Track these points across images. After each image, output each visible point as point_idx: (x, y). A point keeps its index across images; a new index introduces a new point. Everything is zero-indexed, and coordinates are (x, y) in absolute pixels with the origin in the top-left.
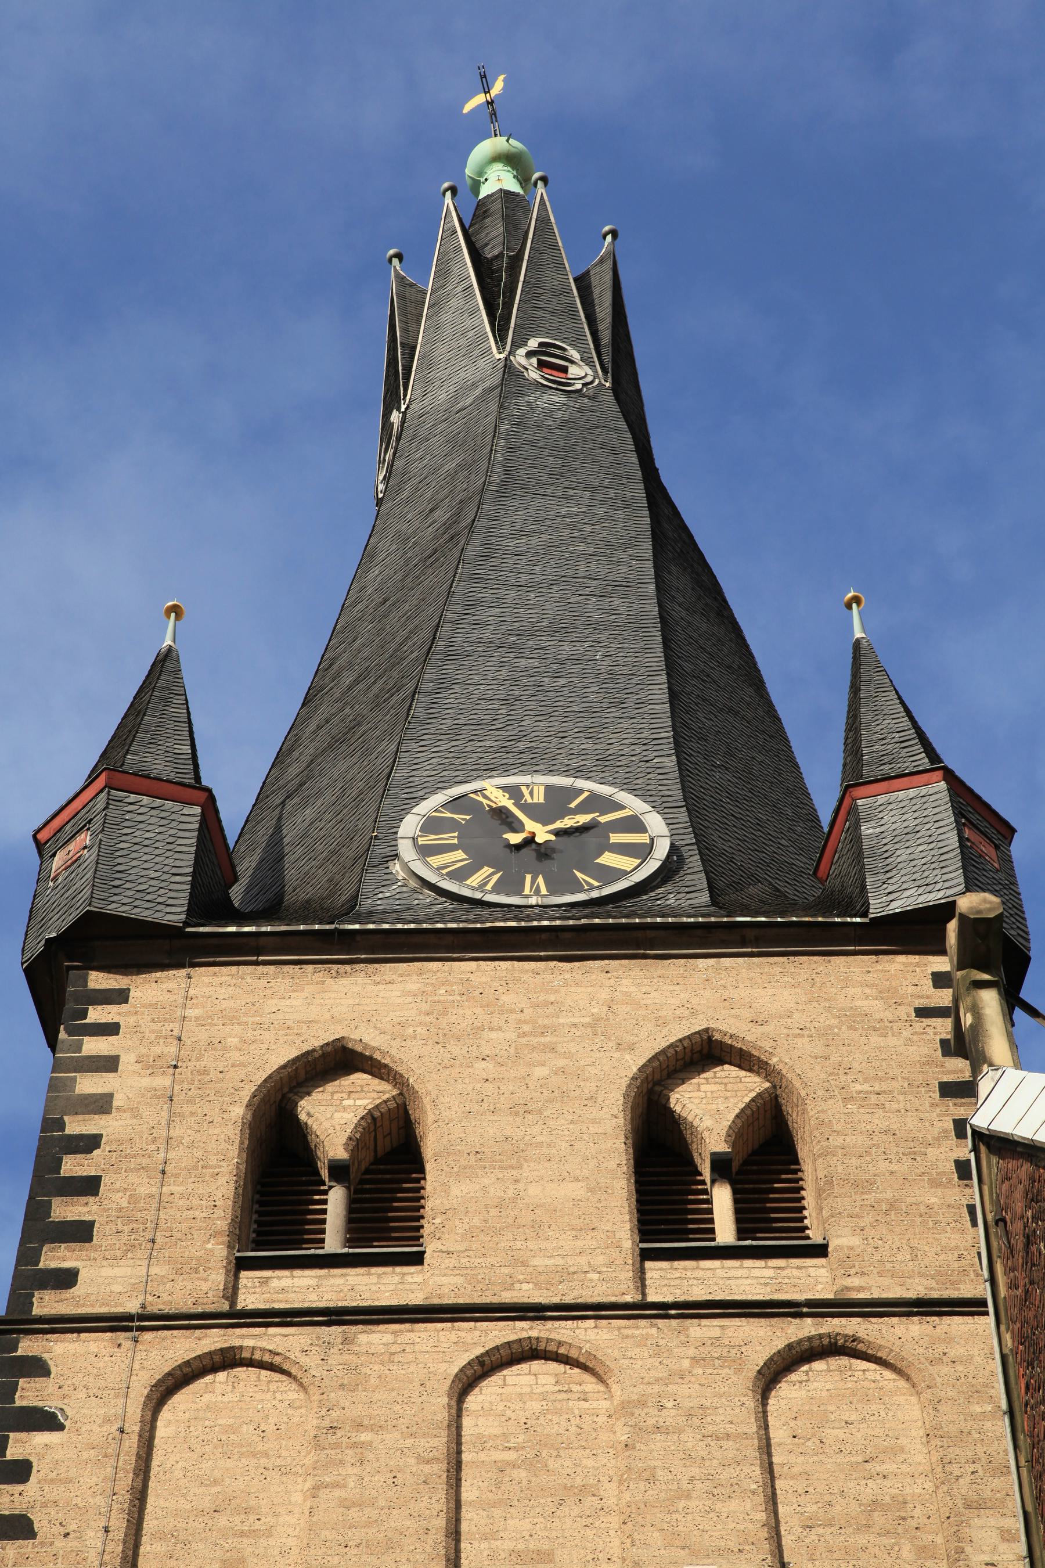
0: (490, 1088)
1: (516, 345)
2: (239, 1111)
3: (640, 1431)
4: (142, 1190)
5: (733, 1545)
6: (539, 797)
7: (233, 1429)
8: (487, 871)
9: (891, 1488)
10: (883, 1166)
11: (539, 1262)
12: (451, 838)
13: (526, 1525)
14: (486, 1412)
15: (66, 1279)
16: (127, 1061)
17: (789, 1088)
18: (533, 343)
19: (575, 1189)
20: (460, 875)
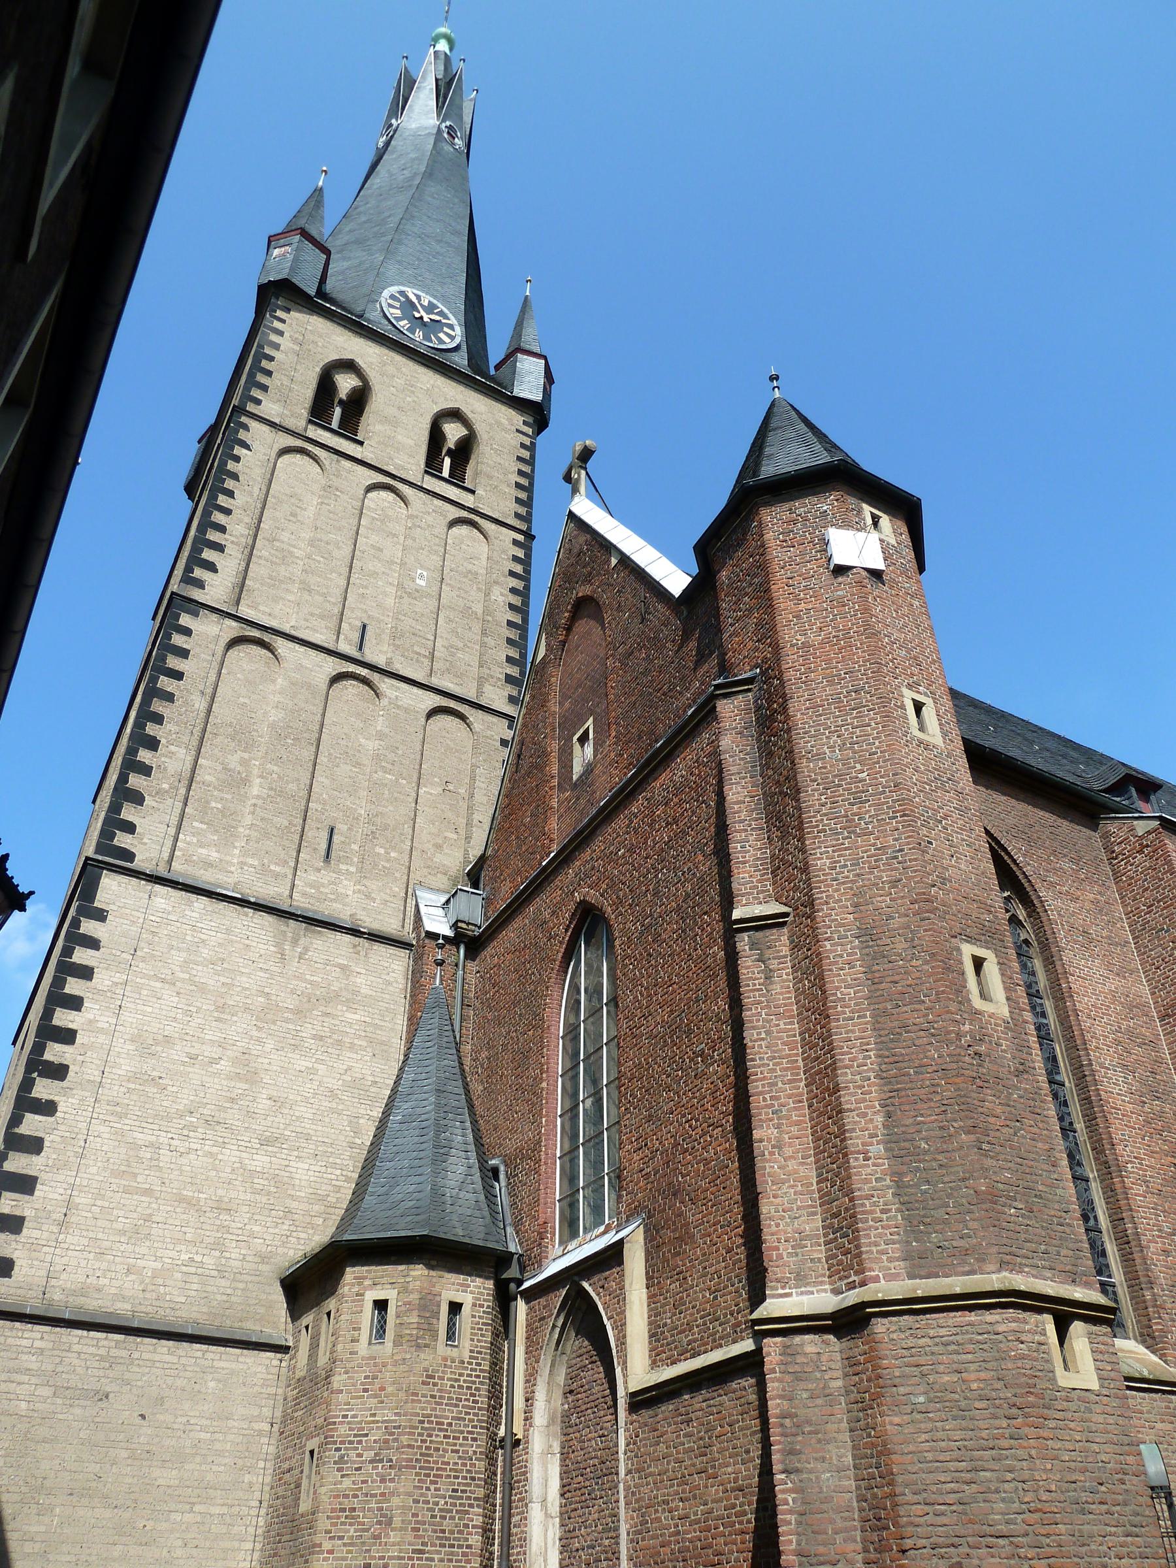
0: (393, 397)
1: (443, 121)
2: (318, 369)
3: (414, 525)
5: (432, 568)
6: (426, 303)
8: (406, 322)
9: (475, 569)
10: (496, 474)
12: (397, 304)
13: (377, 538)
14: (372, 500)
15: (258, 402)
17: (476, 437)
18: (448, 123)
19: (412, 443)
20: (398, 319)
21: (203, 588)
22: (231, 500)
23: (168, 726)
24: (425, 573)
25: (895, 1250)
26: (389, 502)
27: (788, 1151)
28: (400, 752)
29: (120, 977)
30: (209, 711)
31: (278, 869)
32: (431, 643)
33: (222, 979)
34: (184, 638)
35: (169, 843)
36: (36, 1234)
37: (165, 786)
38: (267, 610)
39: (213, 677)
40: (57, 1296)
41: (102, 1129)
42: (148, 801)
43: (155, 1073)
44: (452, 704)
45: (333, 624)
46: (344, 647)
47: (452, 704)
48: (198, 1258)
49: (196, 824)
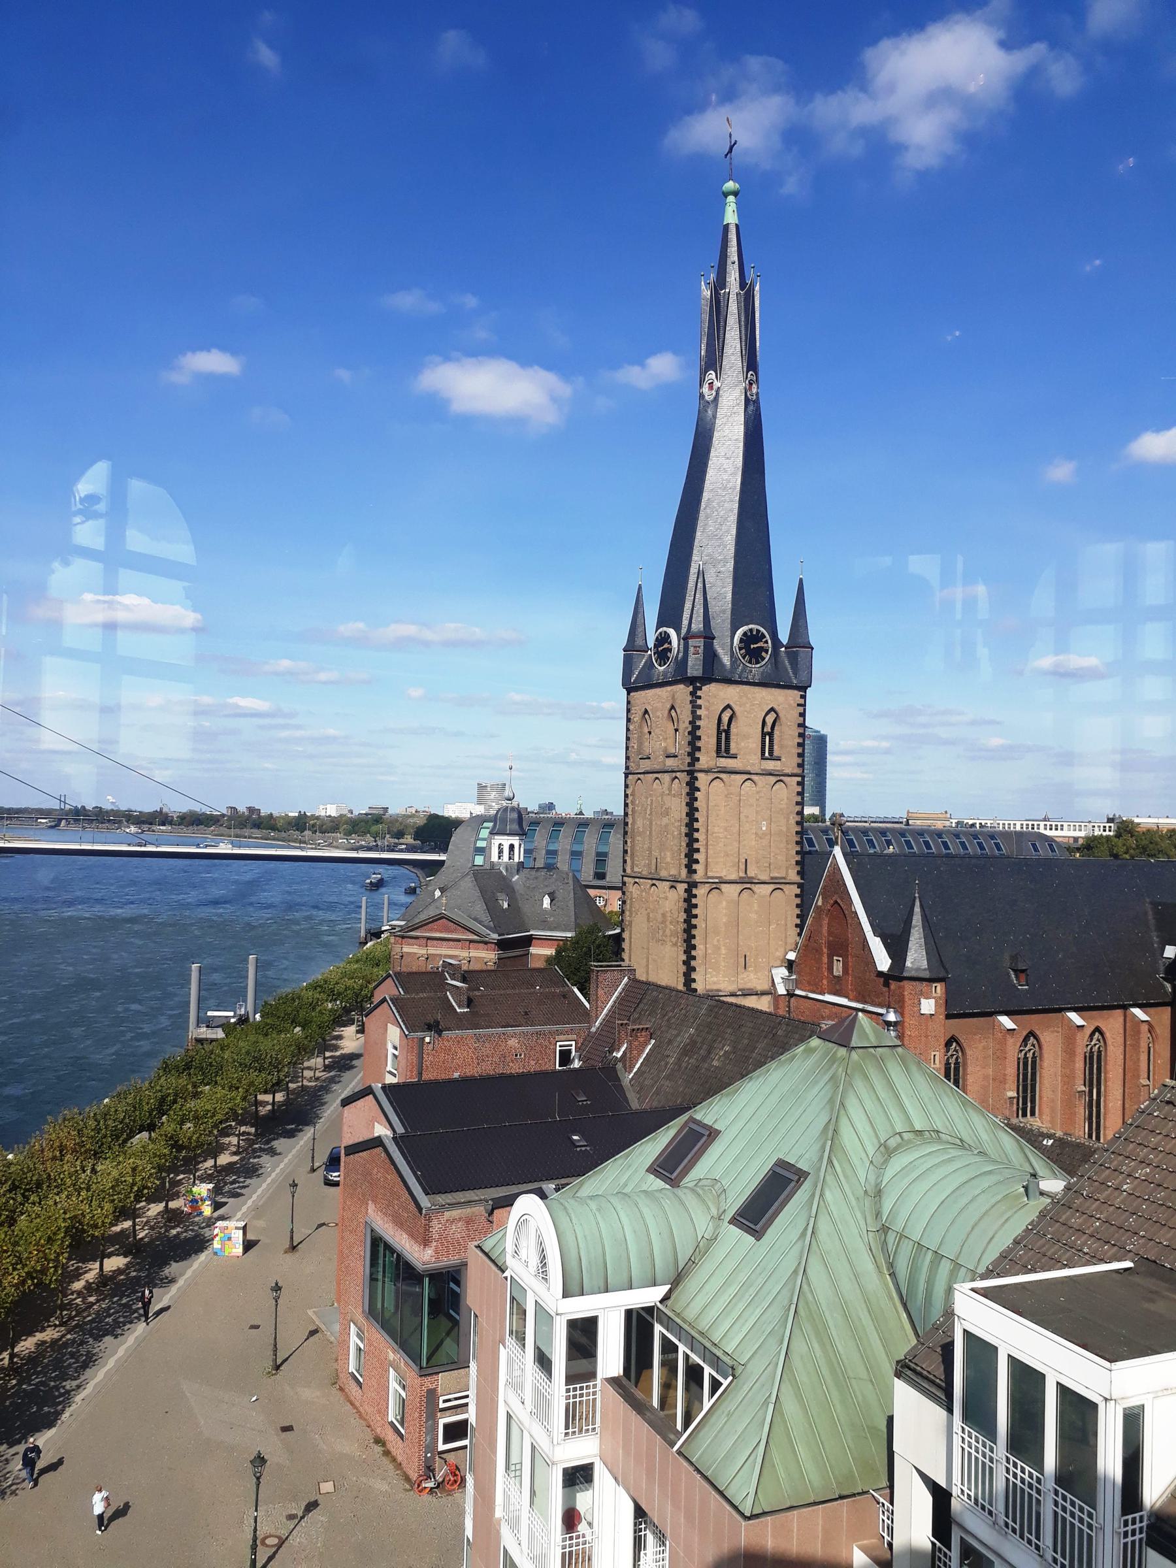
23: (697, 938)
42: (697, 969)
44: (778, 886)
47: (778, 886)
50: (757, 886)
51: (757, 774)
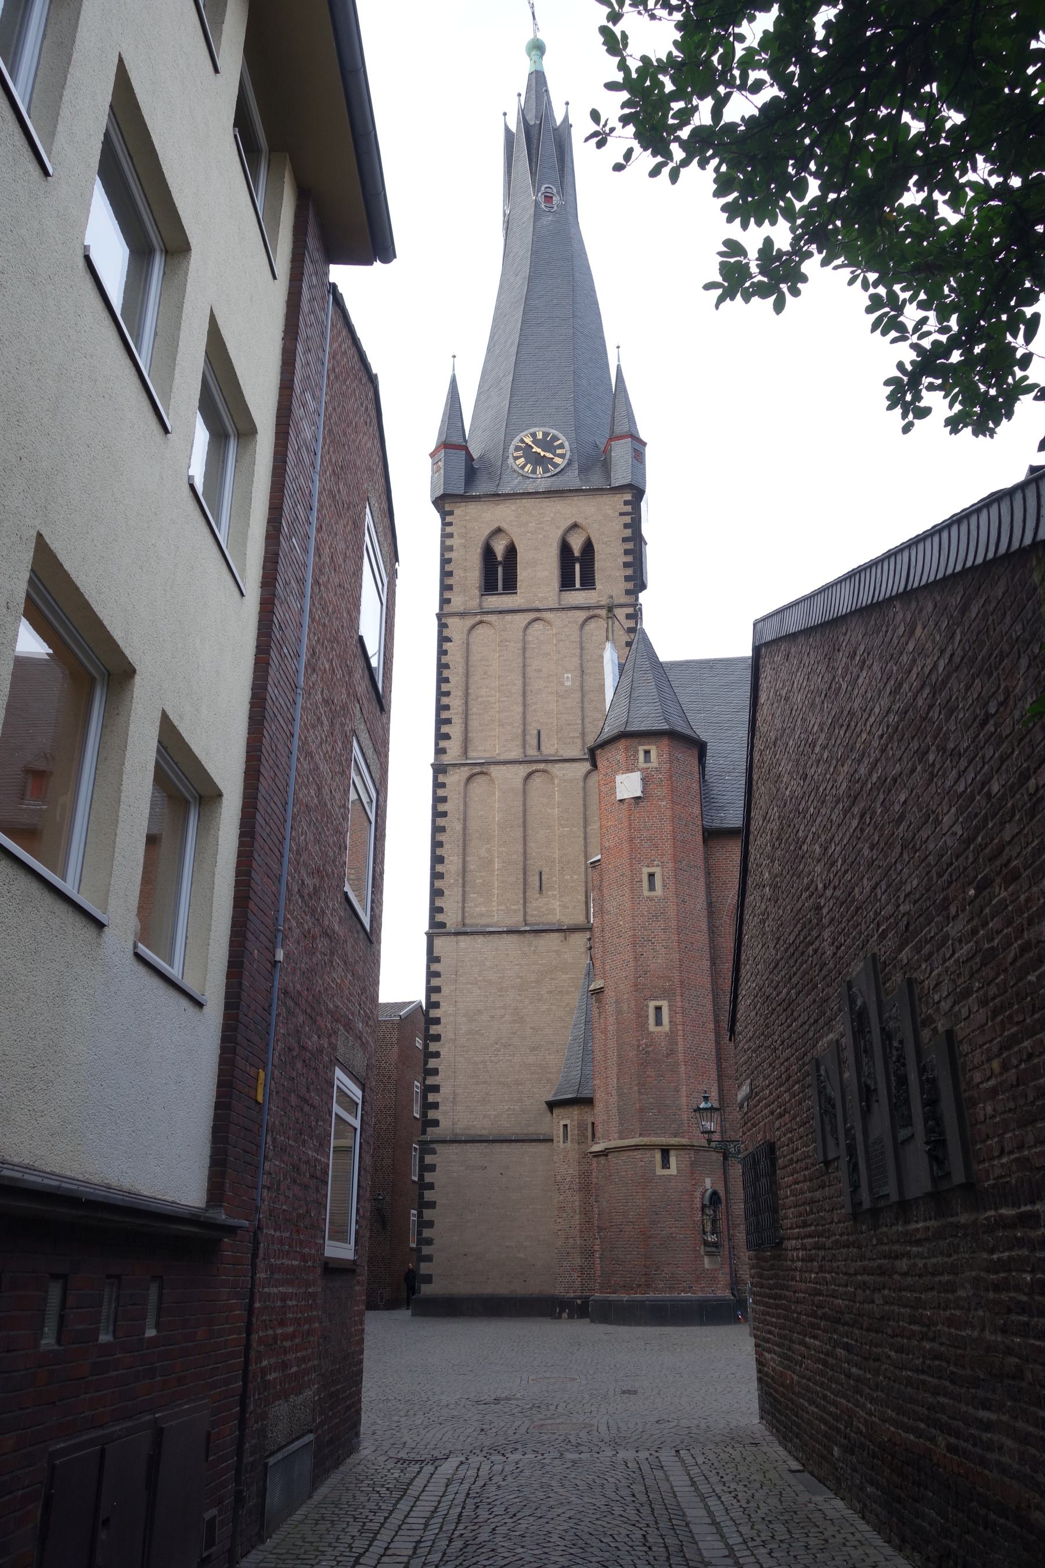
2: (479, 550)
3: (558, 641)
4: (462, 575)
7: (483, 640)
8: (529, 465)
11: (540, 595)
12: (520, 453)
16: (455, 534)
19: (547, 573)
21: (445, 752)
22: (448, 685)
23: (446, 846)
24: (570, 675)
25: (616, 1129)
26: (540, 630)
27: (602, 1089)
28: (571, 811)
29: (453, 987)
30: (465, 828)
31: (515, 907)
32: (580, 726)
33: (498, 975)
34: (443, 789)
35: (460, 912)
36: (444, 1108)
37: (452, 881)
38: (483, 748)
39: (462, 808)
40: (459, 1131)
41: (461, 1059)
42: (446, 893)
43: (477, 1029)
45: (519, 742)
46: (532, 752)
48: (512, 1107)
49: (472, 895)
50: (558, 766)
51: (551, 610)
